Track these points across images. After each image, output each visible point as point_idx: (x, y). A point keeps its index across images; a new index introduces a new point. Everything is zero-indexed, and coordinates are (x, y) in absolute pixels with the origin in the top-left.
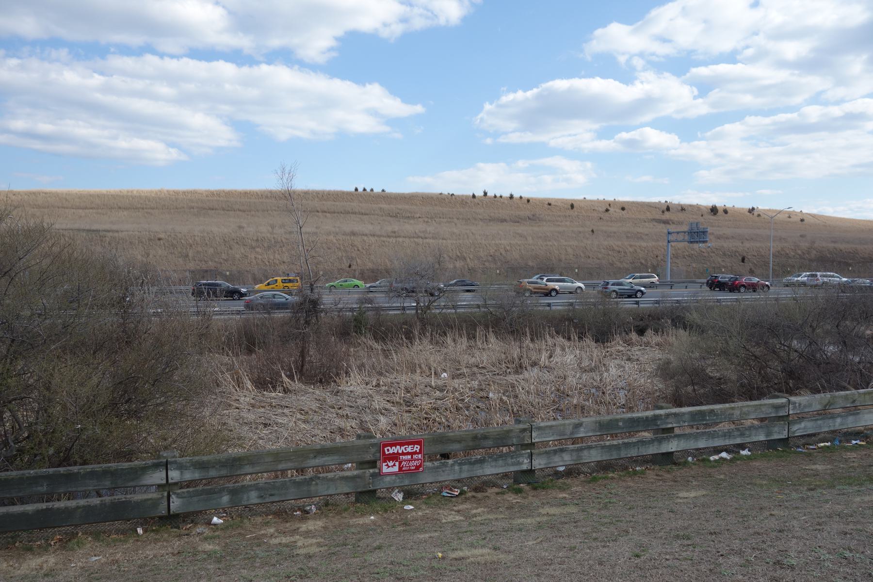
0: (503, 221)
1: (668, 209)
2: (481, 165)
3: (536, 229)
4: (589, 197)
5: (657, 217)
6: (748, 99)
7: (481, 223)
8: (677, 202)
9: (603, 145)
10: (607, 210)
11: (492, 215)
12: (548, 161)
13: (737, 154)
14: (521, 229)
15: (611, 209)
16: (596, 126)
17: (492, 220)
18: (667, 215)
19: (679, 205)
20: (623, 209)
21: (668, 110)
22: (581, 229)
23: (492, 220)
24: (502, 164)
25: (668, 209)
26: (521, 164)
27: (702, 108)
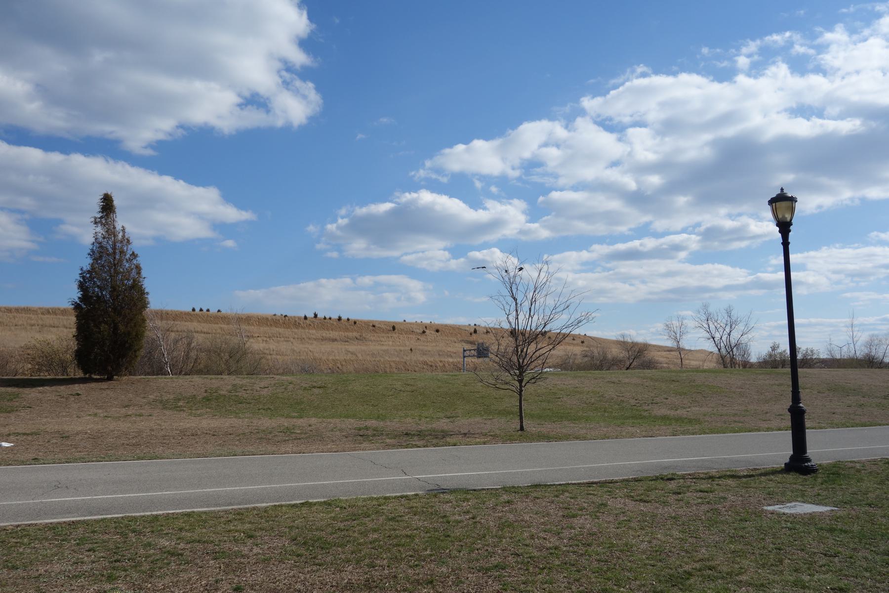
0: (334, 340)
1: (475, 331)
2: (323, 281)
3: (363, 348)
4: (411, 318)
5: (466, 338)
6: (582, 226)
7: (315, 342)
8: (483, 324)
9: (454, 264)
10: (424, 332)
11: (324, 335)
12: (394, 279)
13: (571, 277)
14: (352, 348)
15: (427, 331)
16: (442, 244)
17: (324, 339)
18: (474, 337)
19: (485, 328)
20: (437, 331)
21: (510, 231)
22: (402, 348)
23: (324, 339)
24: (348, 281)
25: (475, 331)
26: (367, 280)
27: (541, 232)
